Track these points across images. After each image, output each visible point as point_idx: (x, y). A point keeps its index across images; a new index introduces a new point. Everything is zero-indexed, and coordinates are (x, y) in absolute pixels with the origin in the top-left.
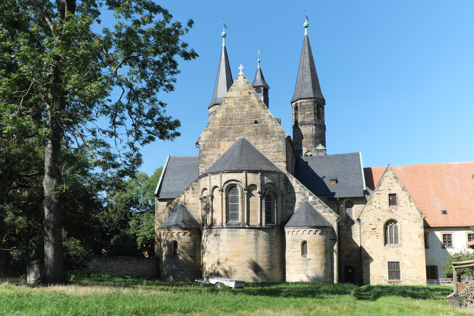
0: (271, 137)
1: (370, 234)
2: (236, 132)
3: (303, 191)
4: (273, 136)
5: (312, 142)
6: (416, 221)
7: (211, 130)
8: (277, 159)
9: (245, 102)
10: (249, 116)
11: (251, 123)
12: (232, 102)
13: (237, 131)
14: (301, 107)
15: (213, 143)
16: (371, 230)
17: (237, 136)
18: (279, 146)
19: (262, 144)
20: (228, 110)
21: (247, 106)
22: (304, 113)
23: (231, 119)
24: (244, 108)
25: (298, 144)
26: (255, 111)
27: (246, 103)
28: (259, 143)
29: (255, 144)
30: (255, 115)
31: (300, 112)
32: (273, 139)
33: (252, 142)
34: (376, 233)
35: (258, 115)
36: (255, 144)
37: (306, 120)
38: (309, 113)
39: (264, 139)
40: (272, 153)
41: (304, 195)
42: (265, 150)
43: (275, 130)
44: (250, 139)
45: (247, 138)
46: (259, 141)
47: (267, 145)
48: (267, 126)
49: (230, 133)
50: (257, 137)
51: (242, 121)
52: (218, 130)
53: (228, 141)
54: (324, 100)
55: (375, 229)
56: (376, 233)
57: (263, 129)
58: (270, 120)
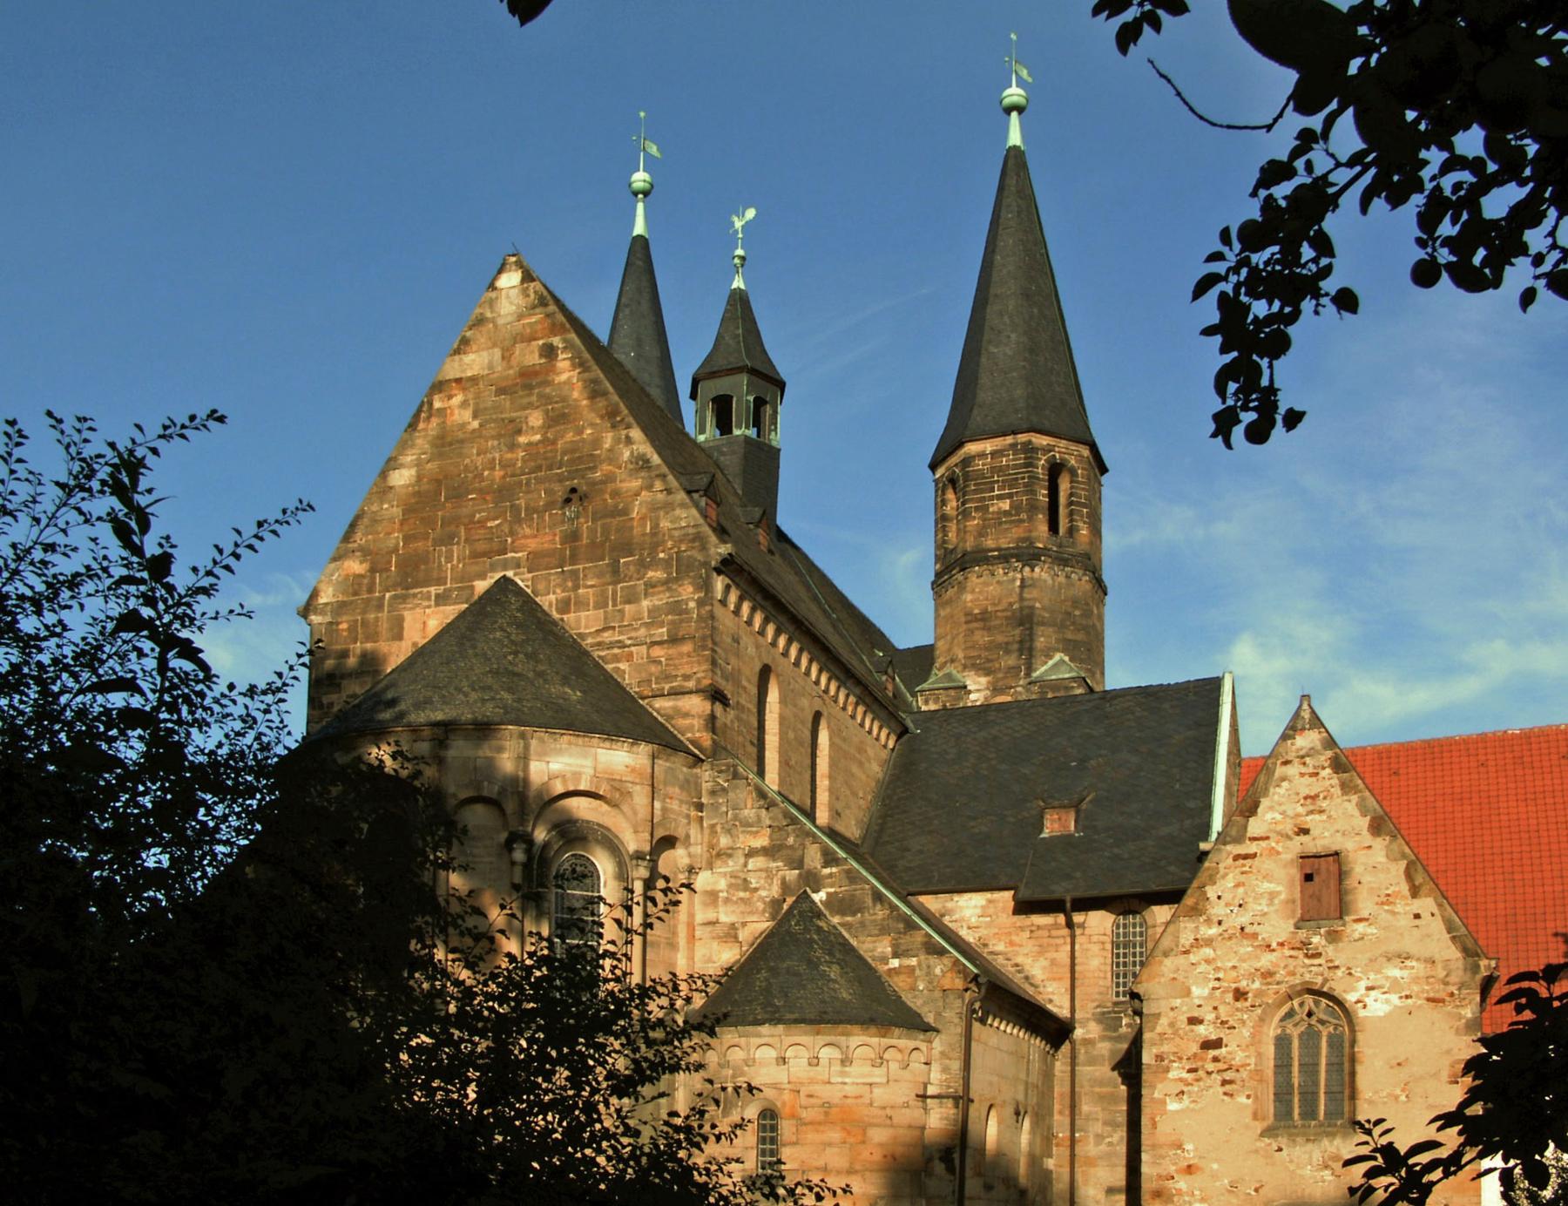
0: (643, 566)
1: (1190, 1071)
2: (475, 555)
3: (791, 840)
4: (654, 563)
6: (1441, 995)
7: (365, 552)
8: (668, 678)
9: (525, 401)
10: (539, 468)
11: (549, 506)
12: (464, 404)
13: (481, 546)
16: (1194, 1048)
17: (483, 577)
18: (677, 608)
19: (596, 608)
20: (446, 443)
21: (536, 419)
24: (519, 432)
26: (570, 436)
27: (530, 406)
28: (581, 605)
29: (564, 606)
30: (572, 461)
32: (650, 574)
33: (548, 601)
34: (1221, 1066)
35: (584, 459)
36: (564, 606)
39: (608, 578)
41: (798, 863)
42: (607, 637)
44: (541, 587)
45: (523, 580)
47: (621, 611)
48: (625, 512)
49: (449, 559)
50: (575, 573)
51: (504, 493)
52: (396, 550)
53: (441, 600)
55: (1218, 1044)
56: (1221, 1066)
58: (636, 484)
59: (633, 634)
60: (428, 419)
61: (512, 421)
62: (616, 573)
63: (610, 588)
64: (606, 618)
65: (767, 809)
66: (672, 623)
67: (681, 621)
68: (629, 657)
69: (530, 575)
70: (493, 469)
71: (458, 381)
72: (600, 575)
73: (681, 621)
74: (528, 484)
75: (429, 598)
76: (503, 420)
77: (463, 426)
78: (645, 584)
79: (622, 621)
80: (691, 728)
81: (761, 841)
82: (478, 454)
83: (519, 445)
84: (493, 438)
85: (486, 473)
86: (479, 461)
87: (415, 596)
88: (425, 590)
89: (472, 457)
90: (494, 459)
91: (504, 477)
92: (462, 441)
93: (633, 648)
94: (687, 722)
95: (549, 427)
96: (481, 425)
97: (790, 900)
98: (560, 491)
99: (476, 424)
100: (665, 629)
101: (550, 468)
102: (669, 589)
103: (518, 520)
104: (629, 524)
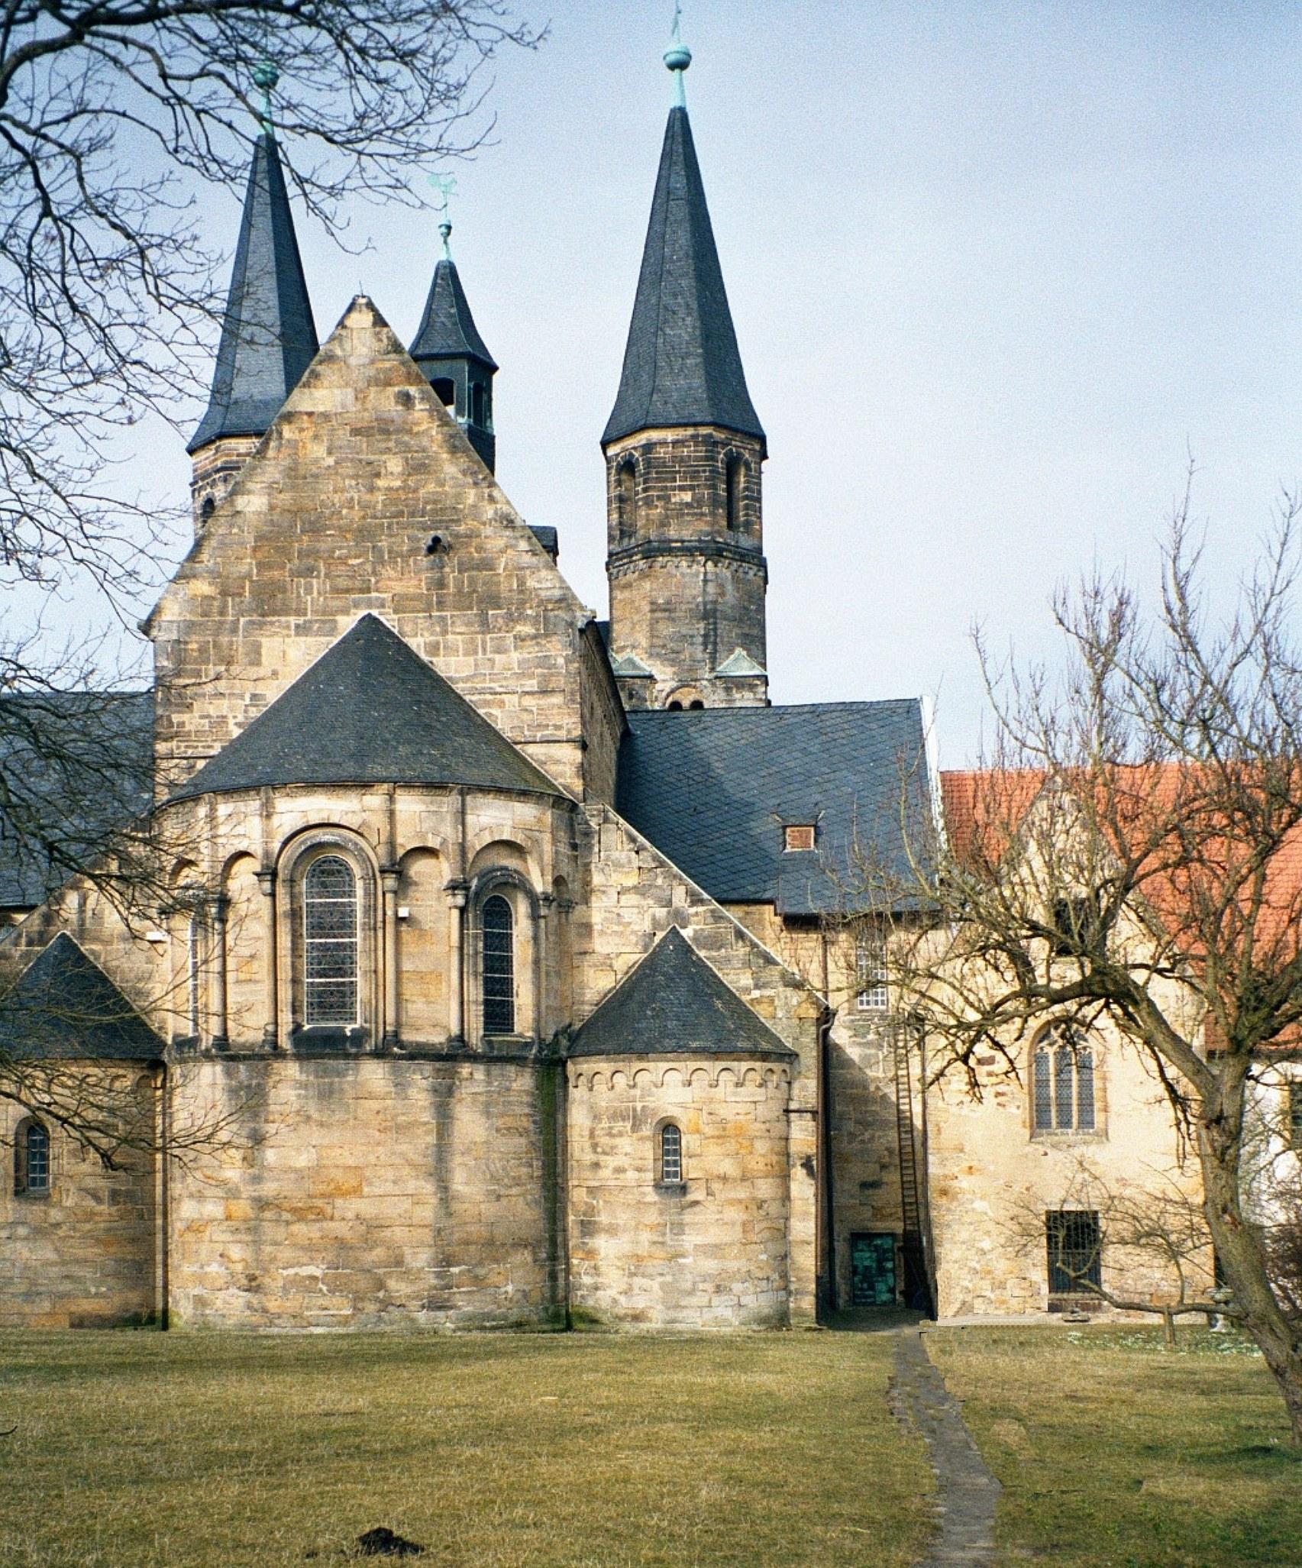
0: (511, 619)
2: (336, 590)
3: (660, 881)
4: (522, 618)
5: (700, 639)
9: (383, 445)
10: (401, 514)
11: (414, 552)
13: (343, 583)
14: (649, 464)
15: (224, 639)
17: (345, 611)
18: (544, 662)
19: (465, 655)
21: (395, 465)
22: (666, 499)
23: (315, 529)
24: (378, 475)
25: (634, 647)
26: (431, 487)
28: (451, 650)
29: (434, 648)
30: (435, 512)
31: (645, 490)
32: (519, 628)
33: (416, 643)
36: (434, 648)
37: (672, 533)
38: (687, 497)
40: (515, 698)
43: (531, 583)
44: (407, 629)
46: (450, 637)
49: (309, 590)
51: (364, 534)
52: (249, 576)
53: (302, 630)
54: (762, 439)
57: (472, 581)
59: (504, 683)
60: (279, 449)
61: (369, 463)
62: (485, 626)
63: (479, 636)
64: (476, 665)
65: (637, 852)
66: (543, 675)
67: (552, 675)
68: (501, 704)
69: (396, 617)
70: (352, 508)
71: (310, 414)
72: (469, 624)
73: (552, 675)
74: (389, 527)
75: (288, 627)
76: (360, 461)
77: (316, 461)
78: (515, 637)
79: (493, 668)
80: (562, 775)
81: (632, 880)
82: (336, 492)
83: (379, 489)
84: (352, 477)
85: (344, 511)
86: (336, 498)
87: (272, 623)
88: (283, 619)
89: (329, 493)
90: (352, 499)
91: (364, 517)
92: (316, 476)
93: (504, 696)
94: (560, 768)
95: (409, 475)
96: (337, 463)
97: (660, 935)
98: (426, 539)
99: (330, 461)
100: (535, 682)
101: (412, 514)
102: (538, 644)
103: (383, 563)
104: (495, 579)
